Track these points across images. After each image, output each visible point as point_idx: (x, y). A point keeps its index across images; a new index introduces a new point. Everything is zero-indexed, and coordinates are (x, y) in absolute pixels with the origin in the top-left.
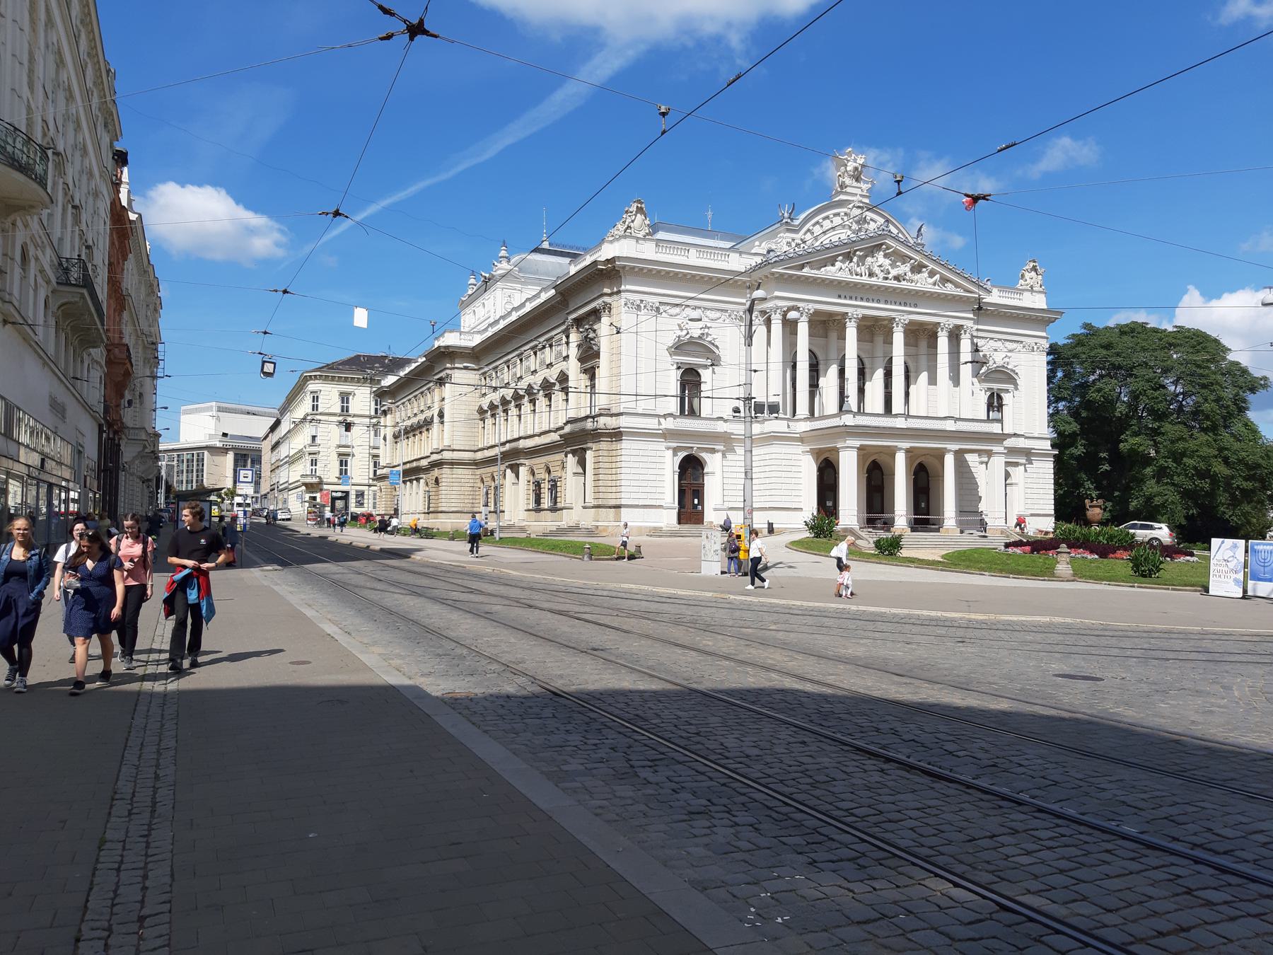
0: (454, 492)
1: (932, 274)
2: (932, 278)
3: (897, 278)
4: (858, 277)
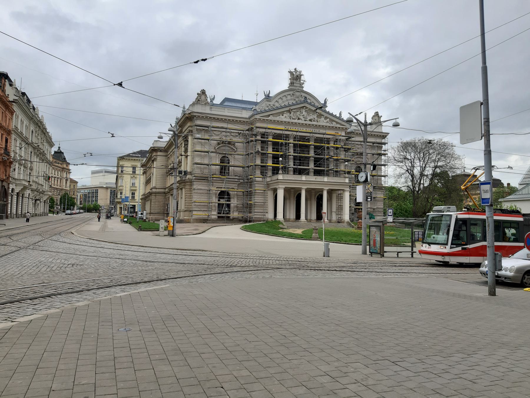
0: (156, 205)
1: (326, 118)
2: (326, 120)
3: (310, 120)
4: (293, 120)
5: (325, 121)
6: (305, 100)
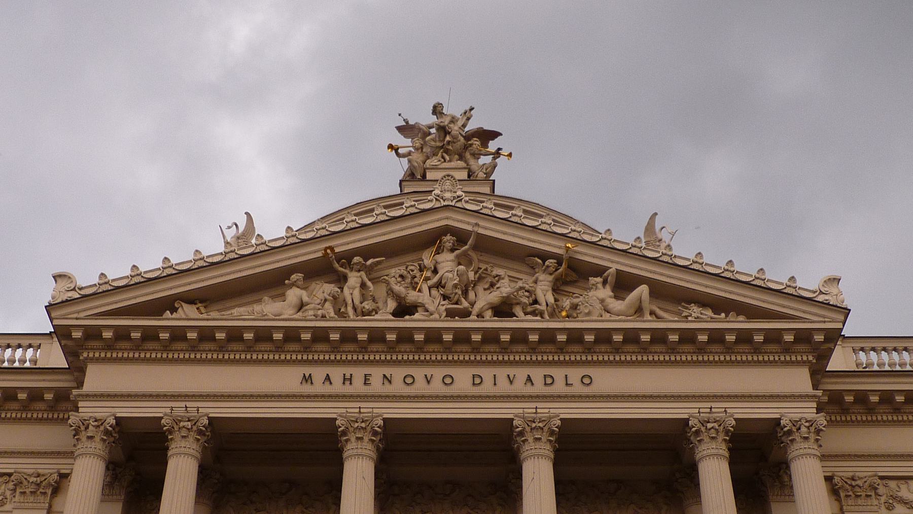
2: (625, 299)
3: (503, 310)
6: (448, 195)
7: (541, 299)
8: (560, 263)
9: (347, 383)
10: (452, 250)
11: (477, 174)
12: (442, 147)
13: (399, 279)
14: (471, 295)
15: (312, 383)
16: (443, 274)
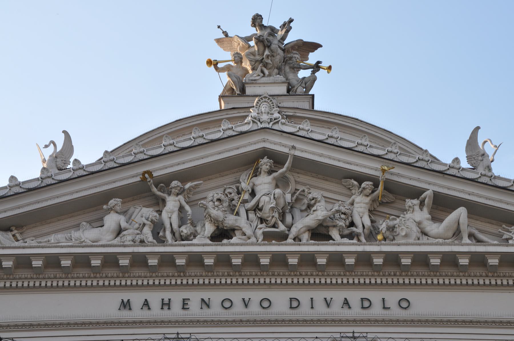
5: (433, 228)
6: (265, 117)
7: (357, 221)
8: (376, 185)
9: (166, 307)
10: (270, 172)
11: (297, 89)
12: (261, 61)
13: (217, 203)
14: (289, 218)
15: (130, 309)
16: (260, 198)
